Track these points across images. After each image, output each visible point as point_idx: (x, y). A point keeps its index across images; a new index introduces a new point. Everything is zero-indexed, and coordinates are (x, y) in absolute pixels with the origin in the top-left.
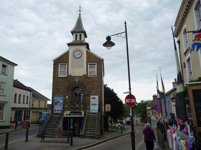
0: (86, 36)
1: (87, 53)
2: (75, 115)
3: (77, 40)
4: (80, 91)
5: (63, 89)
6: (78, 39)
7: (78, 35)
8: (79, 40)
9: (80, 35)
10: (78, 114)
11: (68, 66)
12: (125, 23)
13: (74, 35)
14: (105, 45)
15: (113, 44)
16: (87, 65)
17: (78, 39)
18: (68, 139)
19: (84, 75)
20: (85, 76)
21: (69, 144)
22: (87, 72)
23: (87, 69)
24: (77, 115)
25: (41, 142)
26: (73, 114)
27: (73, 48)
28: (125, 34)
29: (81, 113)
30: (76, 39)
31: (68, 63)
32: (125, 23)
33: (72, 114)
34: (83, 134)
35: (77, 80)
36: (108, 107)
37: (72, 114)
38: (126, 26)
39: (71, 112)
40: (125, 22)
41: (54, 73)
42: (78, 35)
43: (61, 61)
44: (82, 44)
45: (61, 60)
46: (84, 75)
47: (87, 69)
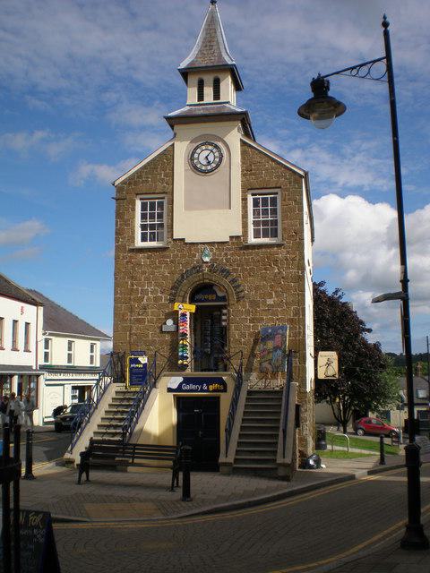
1: (243, 153)
2: (202, 390)
3: (204, 102)
4: (219, 299)
8: (212, 101)
10: (211, 388)
11: (171, 202)
12: (385, 25)
14: (306, 111)
15: (336, 108)
16: (244, 200)
18: (175, 476)
20: (238, 243)
21: (179, 493)
22: (245, 226)
23: (245, 216)
25: (79, 482)
26: (194, 387)
28: (382, 66)
30: (201, 97)
32: (385, 25)
33: (188, 387)
34: (231, 459)
35: (207, 259)
37: (188, 387)
38: (386, 34)
40: (385, 18)
41: (118, 233)
47: (245, 216)
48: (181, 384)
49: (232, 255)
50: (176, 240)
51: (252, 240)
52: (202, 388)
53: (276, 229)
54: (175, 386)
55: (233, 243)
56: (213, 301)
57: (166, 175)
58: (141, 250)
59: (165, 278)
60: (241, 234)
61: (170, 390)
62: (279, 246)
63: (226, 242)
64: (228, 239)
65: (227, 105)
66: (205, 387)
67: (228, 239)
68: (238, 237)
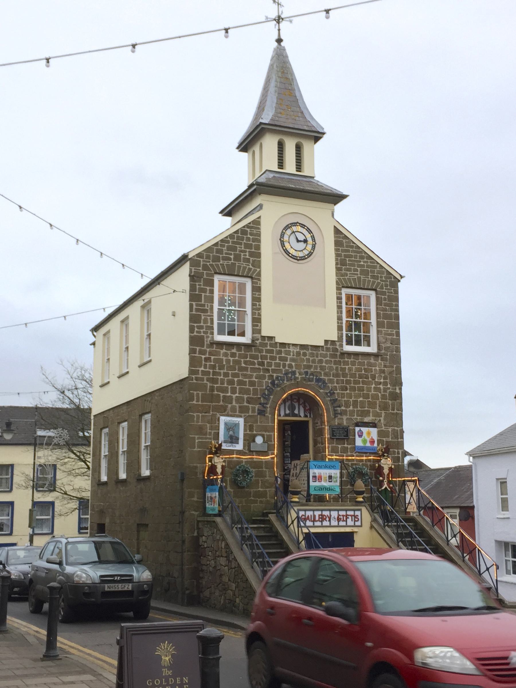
1: (338, 243)
5: (239, 400)
6: (290, 167)
11: (257, 289)
16: (339, 298)
17: (290, 167)
19: (326, 342)
22: (340, 328)
31: (256, 278)
41: (194, 319)
45: (225, 259)
46: (326, 342)
49: (327, 362)
50: (263, 338)
55: (328, 349)
57: (252, 254)
58: (221, 344)
59: (252, 383)
60: (336, 339)
62: (376, 356)
64: (322, 344)
67: (322, 344)
68: (333, 342)
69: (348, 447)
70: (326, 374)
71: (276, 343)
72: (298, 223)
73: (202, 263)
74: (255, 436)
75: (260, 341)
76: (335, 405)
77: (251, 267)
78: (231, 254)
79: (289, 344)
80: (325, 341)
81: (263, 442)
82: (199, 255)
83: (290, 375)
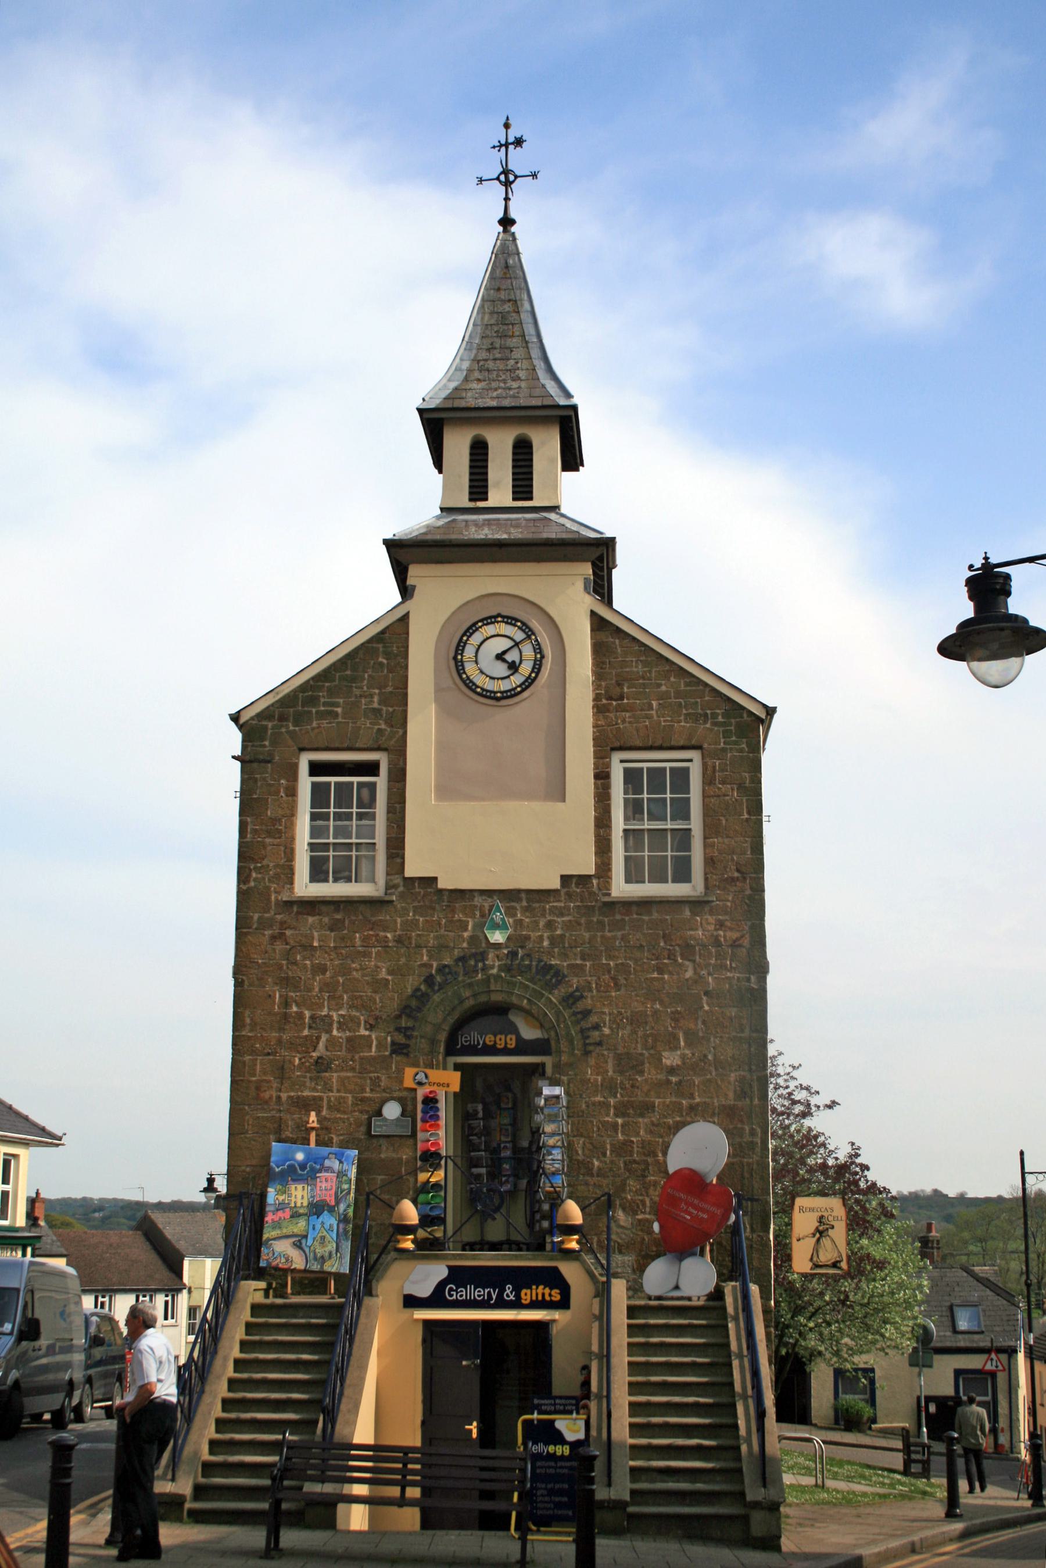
0: (572, 459)
1: (598, 649)
3: (491, 503)
6: (500, 494)
7: (500, 445)
8: (508, 501)
9: (523, 451)
10: (526, 1295)
11: (398, 776)
13: (458, 444)
16: (602, 776)
17: (500, 494)
19: (565, 879)
22: (603, 847)
23: (603, 821)
24: (517, 1305)
26: (478, 1293)
27: (448, 592)
29: (565, 1289)
30: (479, 488)
31: (399, 753)
33: (463, 1294)
35: (497, 937)
36: (821, 1232)
37: (463, 1294)
39: (457, 1276)
41: (247, 855)
42: (500, 445)
43: (317, 738)
44: (548, 543)
46: (565, 879)
47: (603, 821)
48: (441, 1286)
49: (568, 926)
51: (620, 888)
52: (500, 1295)
53: (688, 859)
54: (425, 1291)
56: (506, 1051)
58: (311, 905)
59: (380, 985)
60: (592, 871)
61: (411, 1302)
62: (696, 904)
63: (556, 891)
64: (556, 884)
65: (552, 516)
66: (509, 1293)
67: (556, 884)
68: (583, 880)
69: (616, 1124)
70: (564, 956)
71: (441, 890)
72: (499, 615)
73: (270, 732)
74: (384, 1102)
75: (401, 889)
76: (584, 1025)
77: (383, 726)
78: (337, 705)
79: (471, 891)
80: (562, 877)
81: (403, 1114)
82: (262, 715)
83: (472, 962)
